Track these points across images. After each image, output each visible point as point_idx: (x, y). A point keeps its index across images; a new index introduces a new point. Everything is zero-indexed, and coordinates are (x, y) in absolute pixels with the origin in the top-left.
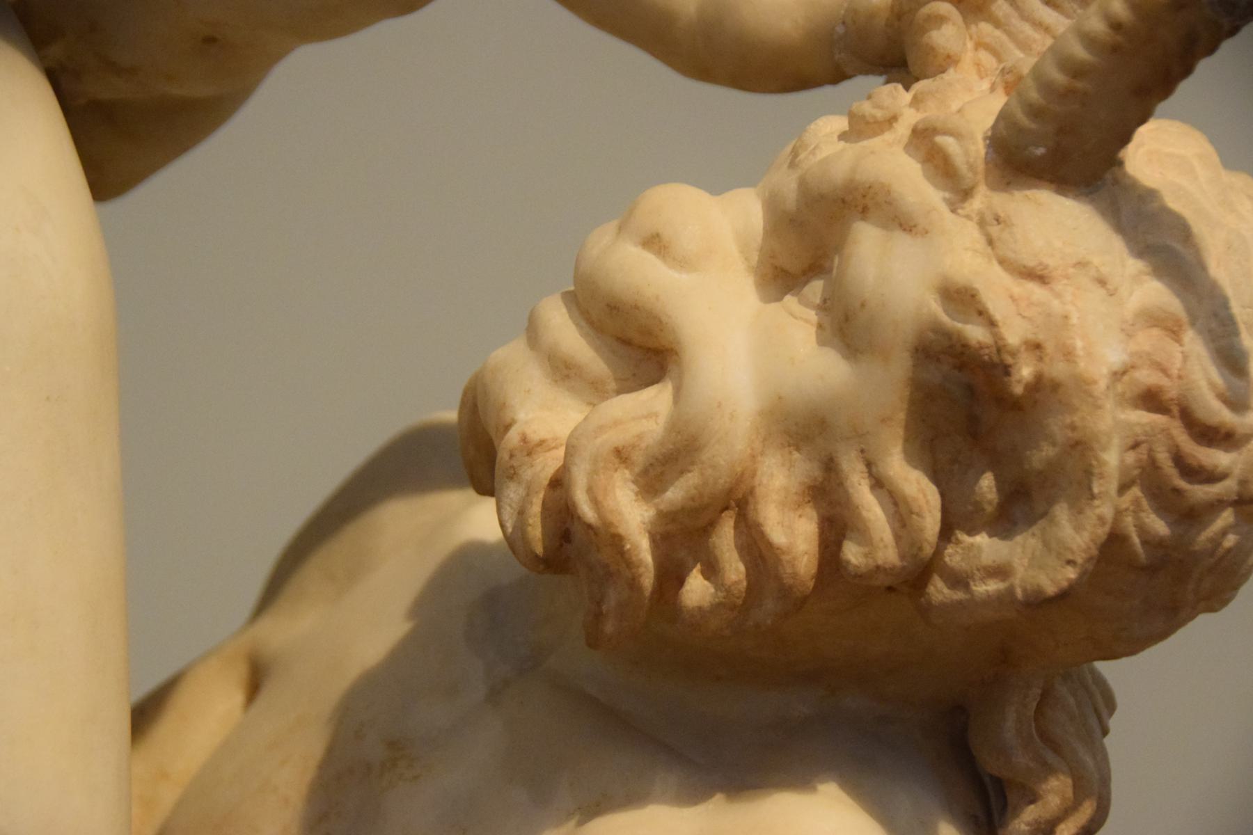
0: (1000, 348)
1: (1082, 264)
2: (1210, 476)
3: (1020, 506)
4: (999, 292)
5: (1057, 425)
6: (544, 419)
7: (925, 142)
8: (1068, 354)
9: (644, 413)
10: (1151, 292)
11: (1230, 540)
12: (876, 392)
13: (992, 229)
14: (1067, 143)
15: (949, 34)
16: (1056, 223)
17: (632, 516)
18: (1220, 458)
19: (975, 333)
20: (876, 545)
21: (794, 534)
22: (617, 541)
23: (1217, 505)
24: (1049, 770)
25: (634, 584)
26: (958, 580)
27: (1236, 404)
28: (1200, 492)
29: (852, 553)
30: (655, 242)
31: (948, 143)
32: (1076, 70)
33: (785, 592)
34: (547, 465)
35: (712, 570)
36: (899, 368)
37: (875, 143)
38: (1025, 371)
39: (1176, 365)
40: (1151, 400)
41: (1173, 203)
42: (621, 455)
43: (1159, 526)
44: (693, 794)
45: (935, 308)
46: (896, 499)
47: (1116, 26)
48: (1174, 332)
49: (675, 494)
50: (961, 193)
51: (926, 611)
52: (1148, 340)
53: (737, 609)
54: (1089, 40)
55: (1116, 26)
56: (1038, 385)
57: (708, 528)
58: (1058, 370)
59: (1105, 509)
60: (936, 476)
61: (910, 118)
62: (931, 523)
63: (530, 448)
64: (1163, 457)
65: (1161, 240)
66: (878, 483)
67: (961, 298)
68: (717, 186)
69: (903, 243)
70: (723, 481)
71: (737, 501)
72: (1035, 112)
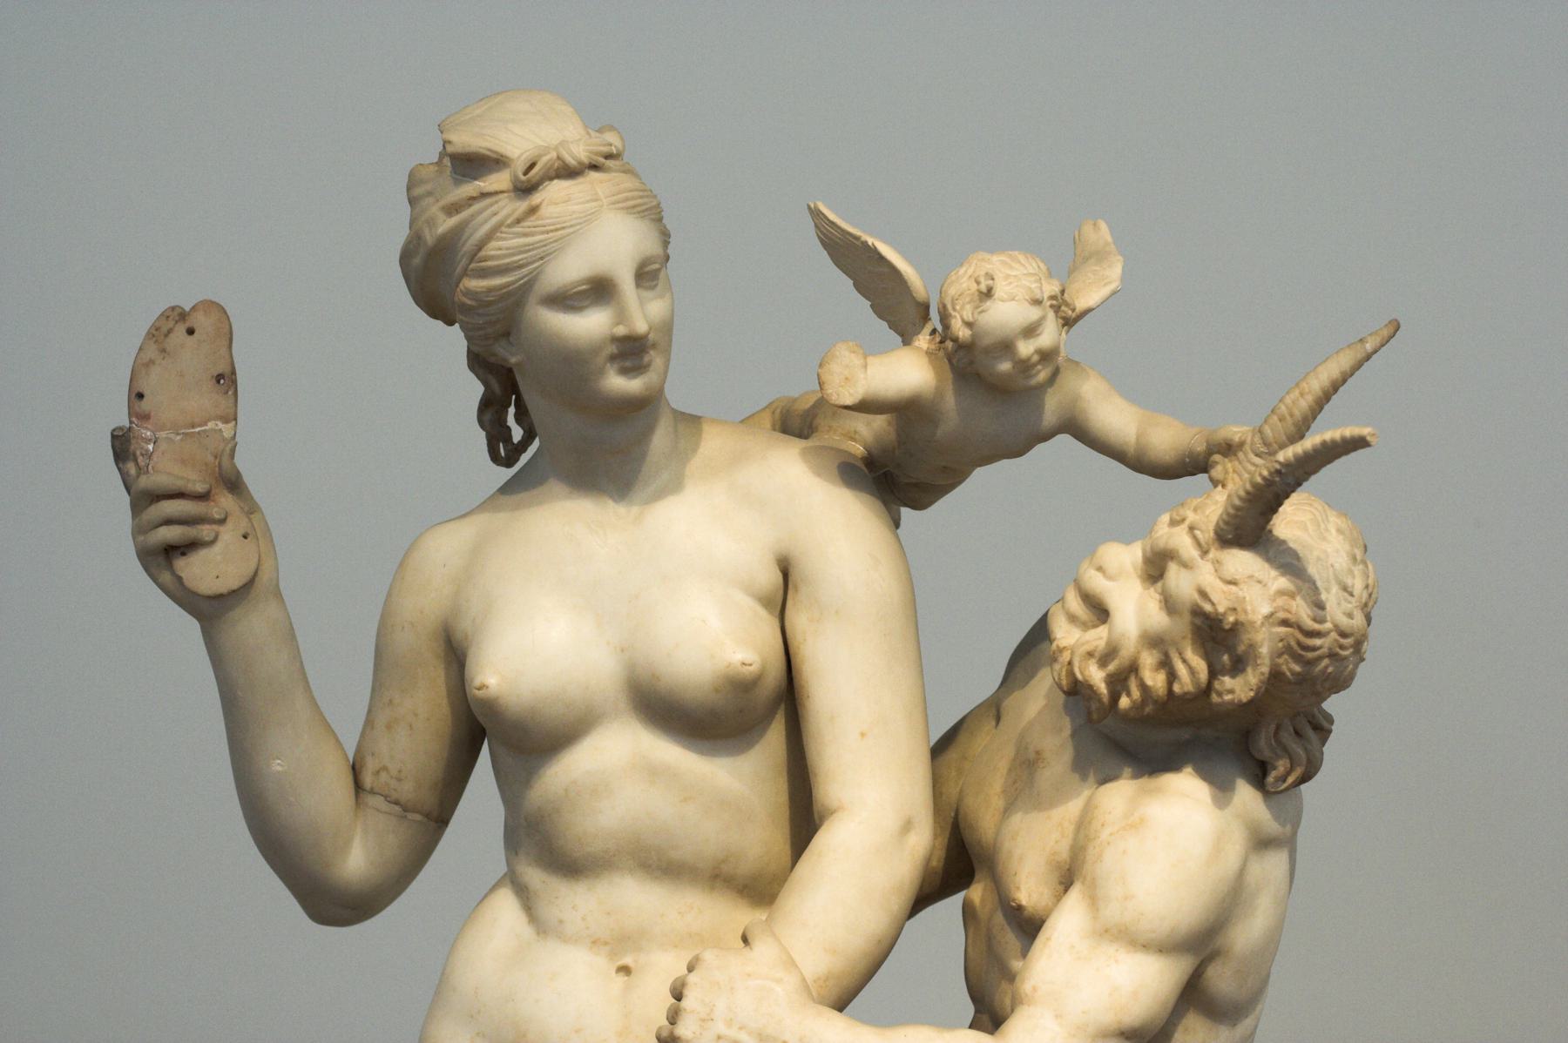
0: (1217, 613)
1: (1251, 577)
2: (1314, 649)
3: (1238, 666)
5: (1245, 638)
6: (1065, 634)
8: (1245, 612)
9: (1098, 637)
10: (1283, 582)
11: (1330, 670)
12: (1181, 627)
13: (1217, 563)
14: (1249, 527)
16: (1242, 562)
17: (1097, 677)
18: (1317, 642)
19: (1208, 608)
20: (1185, 683)
21: (1155, 680)
22: (1090, 687)
23: (1320, 658)
24: (1278, 757)
25: (1100, 700)
26: (1220, 694)
27: (1321, 621)
28: (1310, 655)
29: (1176, 688)
30: (1100, 569)
31: (1197, 532)
32: (1237, 509)
33: (1156, 702)
34: (1066, 656)
35: (1129, 695)
36: (1187, 618)
37: (1177, 530)
38: (1231, 619)
39: (1294, 609)
40: (1285, 623)
41: (1292, 545)
42: (1090, 654)
43: (1297, 668)
44: (1136, 776)
45: (1196, 596)
46: (1192, 667)
47: (1248, 493)
48: (1292, 596)
49: (1112, 667)
50: (1204, 553)
51: (1211, 704)
52: (1280, 601)
53: (1138, 706)
54: (1240, 498)
55: (1248, 493)
56: (1236, 623)
57: (1126, 679)
58: (1242, 618)
59: (1265, 669)
62: (1203, 675)
63: (1061, 650)
64: (1293, 643)
65: (1288, 561)
66: (1184, 661)
67: (1203, 594)
68: (1128, 542)
70: (1127, 663)
71: (1133, 668)
72: (1227, 523)
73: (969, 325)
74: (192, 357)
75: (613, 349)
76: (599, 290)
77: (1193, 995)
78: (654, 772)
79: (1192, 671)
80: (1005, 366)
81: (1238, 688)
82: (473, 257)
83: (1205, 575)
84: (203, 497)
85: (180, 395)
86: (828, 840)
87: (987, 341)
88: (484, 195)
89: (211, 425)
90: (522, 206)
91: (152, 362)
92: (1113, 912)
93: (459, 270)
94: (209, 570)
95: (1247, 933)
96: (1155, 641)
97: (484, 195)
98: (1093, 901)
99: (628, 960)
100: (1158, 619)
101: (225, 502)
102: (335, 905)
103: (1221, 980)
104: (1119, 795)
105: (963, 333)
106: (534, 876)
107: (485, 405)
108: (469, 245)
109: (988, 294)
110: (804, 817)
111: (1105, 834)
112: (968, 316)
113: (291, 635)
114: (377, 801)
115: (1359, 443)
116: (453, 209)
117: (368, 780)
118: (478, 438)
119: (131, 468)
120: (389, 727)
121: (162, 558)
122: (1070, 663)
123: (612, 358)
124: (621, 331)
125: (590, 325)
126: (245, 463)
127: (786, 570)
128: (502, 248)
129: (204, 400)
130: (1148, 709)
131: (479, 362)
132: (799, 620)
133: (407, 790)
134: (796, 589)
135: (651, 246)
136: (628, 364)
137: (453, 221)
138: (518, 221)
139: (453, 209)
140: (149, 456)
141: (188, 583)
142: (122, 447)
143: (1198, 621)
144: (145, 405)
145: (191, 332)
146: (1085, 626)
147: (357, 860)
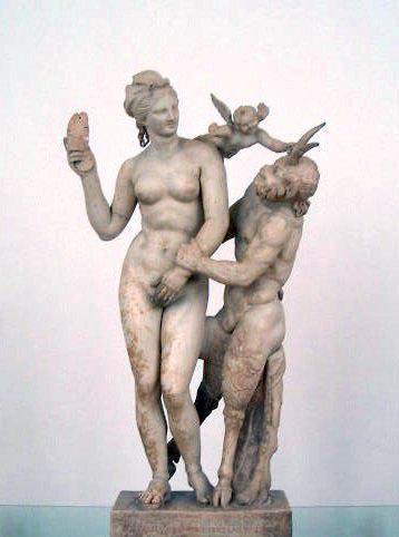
16: (293, 169)
76: (164, 110)
77: (280, 255)
78: (174, 209)
81: (289, 195)
86: (208, 224)
94: (84, 166)
95: (290, 246)
96: (273, 184)
102: (106, 236)
103: (287, 255)
107: (140, 134)
110: (201, 219)
113: (98, 181)
118: (138, 141)
121: (74, 164)
125: (163, 117)
131: (138, 126)
132: (202, 179)
133: (122, 214)
135: (172, 102)
142: (65, 141)
147: (112, 227)
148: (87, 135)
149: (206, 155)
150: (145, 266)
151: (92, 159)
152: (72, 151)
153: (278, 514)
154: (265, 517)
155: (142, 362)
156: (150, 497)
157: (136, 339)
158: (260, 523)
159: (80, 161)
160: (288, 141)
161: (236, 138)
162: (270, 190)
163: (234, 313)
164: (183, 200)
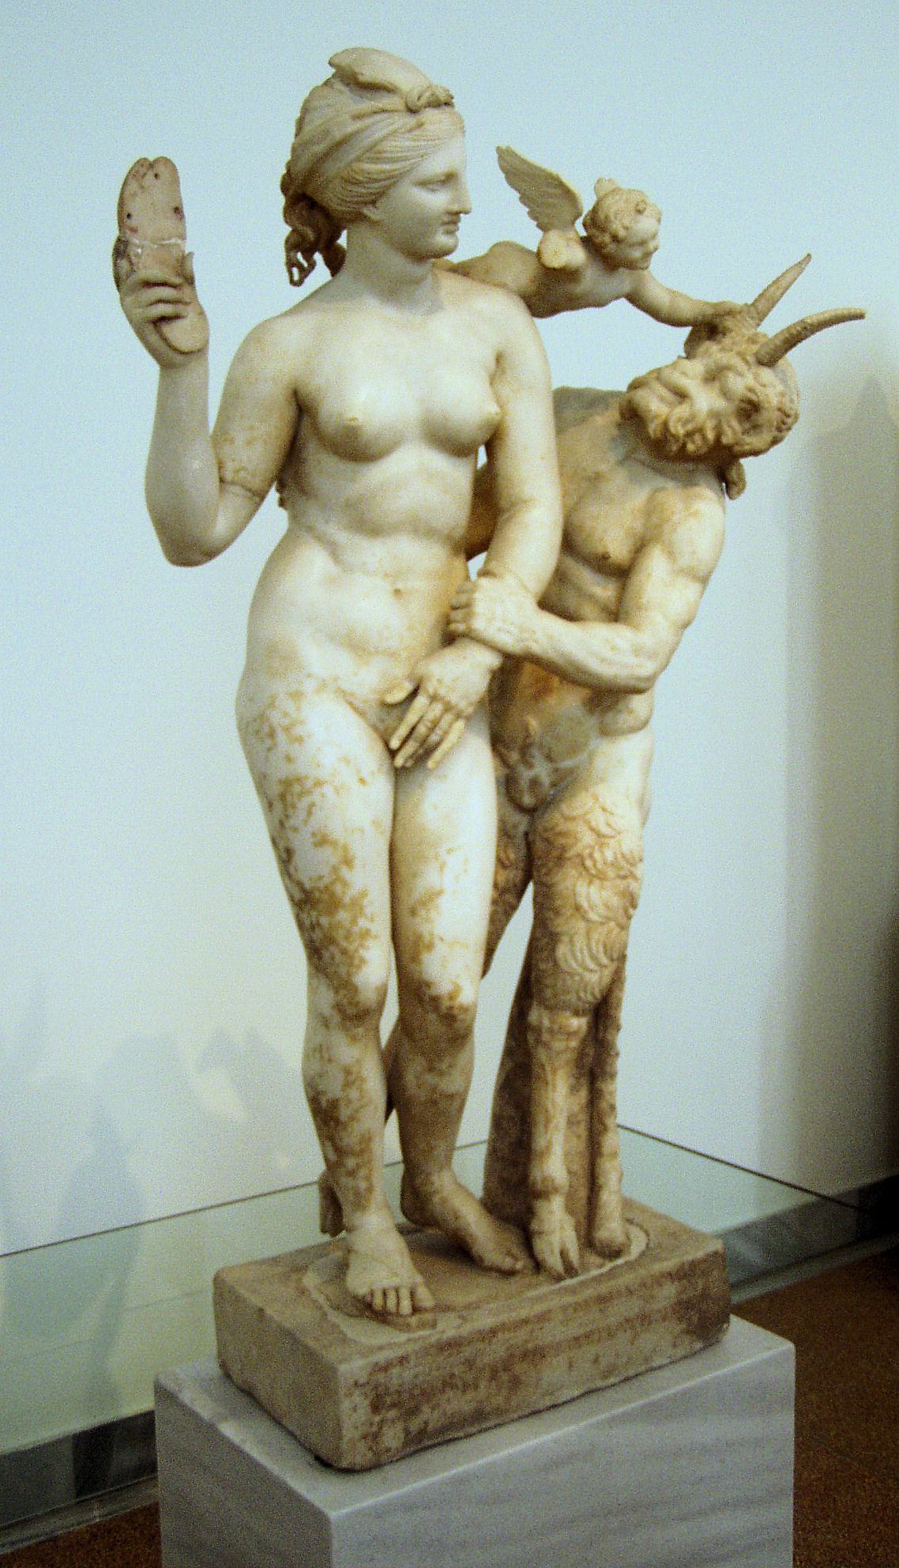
3: (756, 427)
4: (758, 388)
7: (739, 354)
9: (682, 411)
10: (780, 388)
13: (756, 377)
15: (729, 322)
16: (766, 374)
19: (754, 398)
20: (726, 440)
21: (711, 436)
30: (684, 373)
40: (779, 409)
42: (679, 420)
49: (689, 427)
60: (740, 422)
61: (736, 349)
63: (656, 416)
67: (751, 390)
69: (739, 379)
71: (700, 430)
73: (627, 228)
74: (157, 191)
75: (446, 219)
79: (735, 432)
80: (637, 254)
82: (370, 149)
83: (749, 380)
84: (174, 286)
85: (149, 221)
87: (635, 240)
88: (384, 111)
89: (173, 241)
90: (411, 121)
91: (135, 194)
92: (684, 561)
93: (352, 157)
96: (715, 415)
97: (384, 111)
98: (671, 554)
99: (400, 586)
100: (720, 404)
101: (187, 289)
104: (673, 496)
105: (622, 233)
106: (342, 537)
108: (367, 142)
109: (639, 212)
111: (675, 518)
112: (626, 222)
114: (237, 489)
115: (860, 316)
116: (358, 117)
117: (229, 476)
119: (124, 264)
120: (249, 443)
122: (665, 424)
123: (444, 224)
124: (455, 208)
125: (437, 201)
126: (199, 269)
127: (499, 359)
128: (392, 146)
129: (169, 223)
130: (704, 450)
134: (503, 372)
136: (451, 227)
137: (358, 125)
138: (410, 131)
139: (358, 117)
140: (137, 255)
141: (176, 344)
142: (121, 250)
143: (743, 405)
144: (133, 222)
145: (156, 176)
146: (671, 405)
148: (183, 237)
149: (499, 313)
150: (357, 645)
151: (202, 313)
152: (148, 284)
153: (704, 1261)
154: (671, 1276)
155: (363, 923)
156: (405, 1294)
157: (348, 862)
158: (669, 1292)
159: (177, 317)
160: (713, 299)
161: (592, 278)
162: (700, 430)
163: (549, 758)
164: (459, 449)
